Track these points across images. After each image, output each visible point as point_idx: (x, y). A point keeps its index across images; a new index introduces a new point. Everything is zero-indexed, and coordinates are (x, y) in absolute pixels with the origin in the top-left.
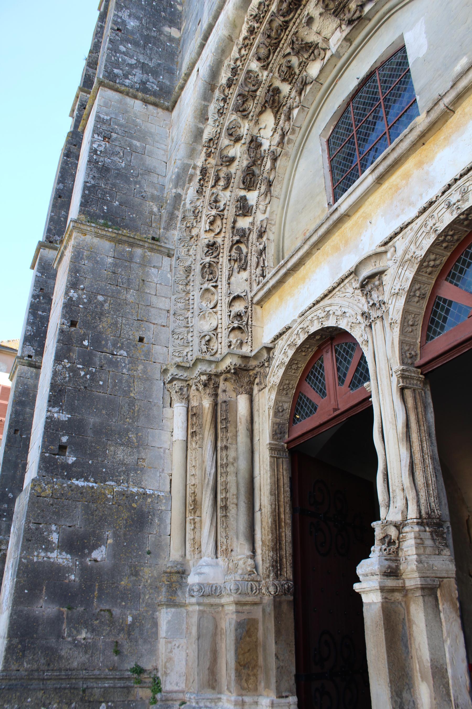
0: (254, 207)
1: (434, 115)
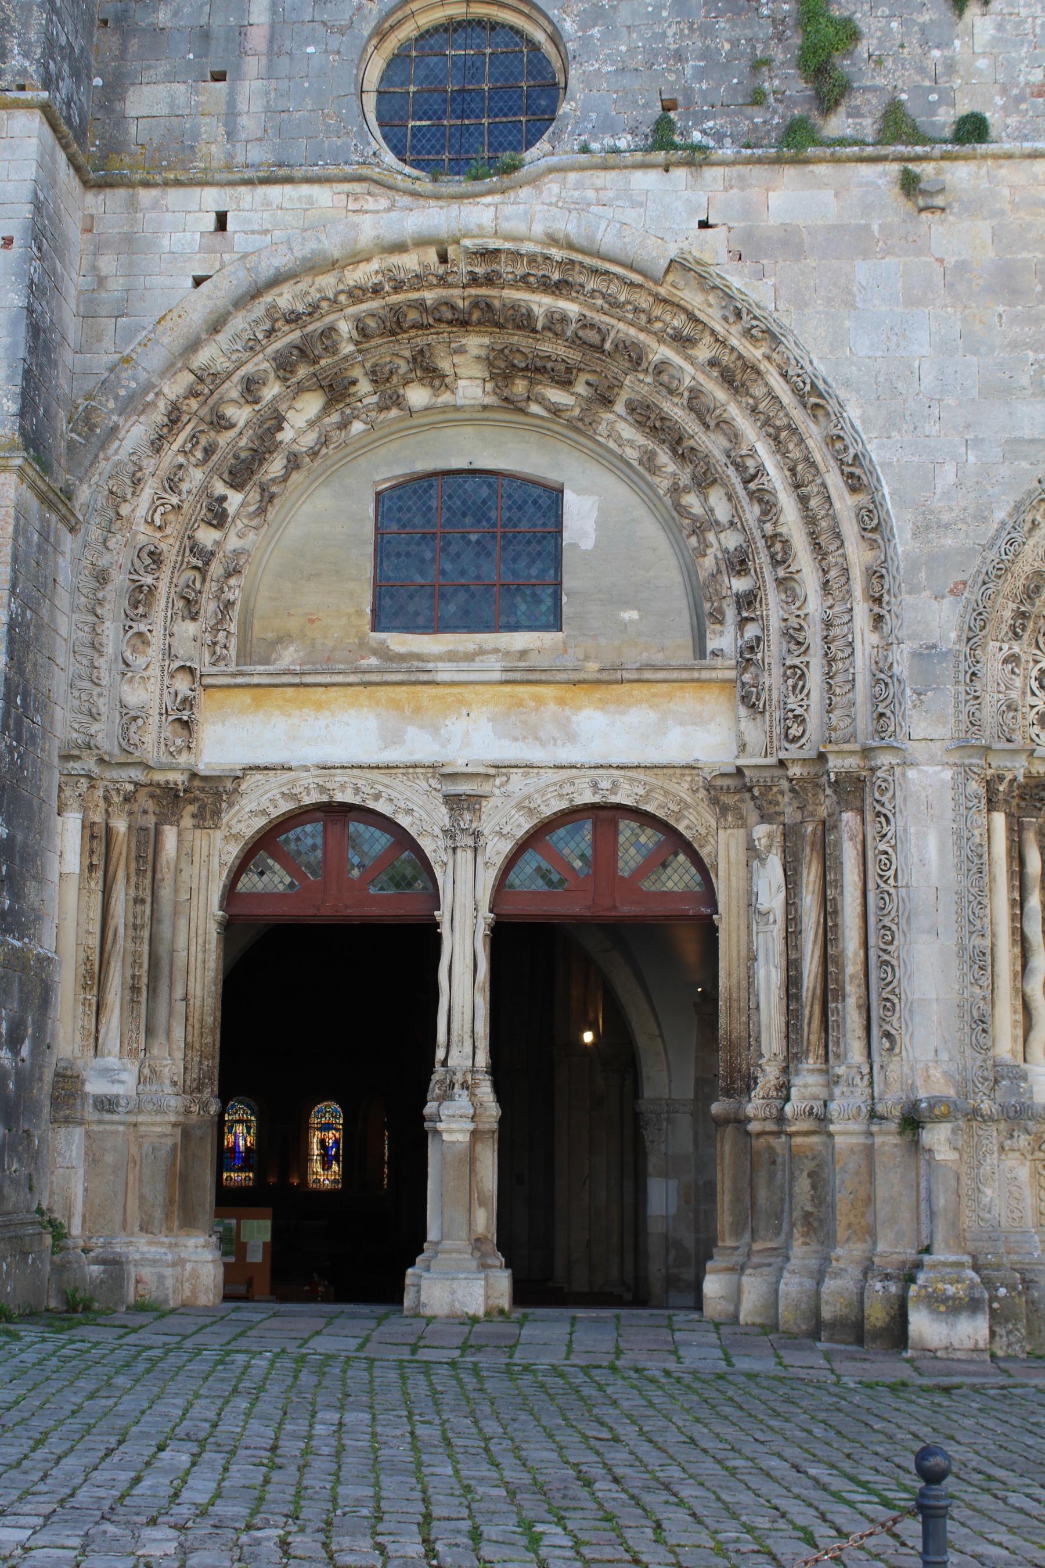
0: (230, 519)
1: (605, 676)
